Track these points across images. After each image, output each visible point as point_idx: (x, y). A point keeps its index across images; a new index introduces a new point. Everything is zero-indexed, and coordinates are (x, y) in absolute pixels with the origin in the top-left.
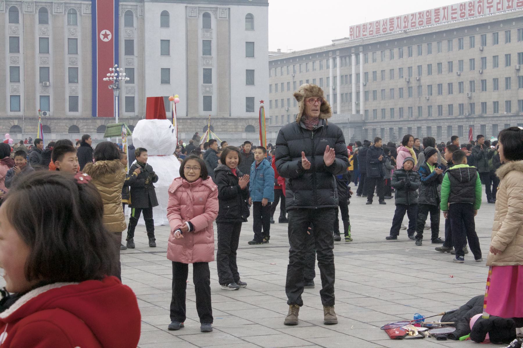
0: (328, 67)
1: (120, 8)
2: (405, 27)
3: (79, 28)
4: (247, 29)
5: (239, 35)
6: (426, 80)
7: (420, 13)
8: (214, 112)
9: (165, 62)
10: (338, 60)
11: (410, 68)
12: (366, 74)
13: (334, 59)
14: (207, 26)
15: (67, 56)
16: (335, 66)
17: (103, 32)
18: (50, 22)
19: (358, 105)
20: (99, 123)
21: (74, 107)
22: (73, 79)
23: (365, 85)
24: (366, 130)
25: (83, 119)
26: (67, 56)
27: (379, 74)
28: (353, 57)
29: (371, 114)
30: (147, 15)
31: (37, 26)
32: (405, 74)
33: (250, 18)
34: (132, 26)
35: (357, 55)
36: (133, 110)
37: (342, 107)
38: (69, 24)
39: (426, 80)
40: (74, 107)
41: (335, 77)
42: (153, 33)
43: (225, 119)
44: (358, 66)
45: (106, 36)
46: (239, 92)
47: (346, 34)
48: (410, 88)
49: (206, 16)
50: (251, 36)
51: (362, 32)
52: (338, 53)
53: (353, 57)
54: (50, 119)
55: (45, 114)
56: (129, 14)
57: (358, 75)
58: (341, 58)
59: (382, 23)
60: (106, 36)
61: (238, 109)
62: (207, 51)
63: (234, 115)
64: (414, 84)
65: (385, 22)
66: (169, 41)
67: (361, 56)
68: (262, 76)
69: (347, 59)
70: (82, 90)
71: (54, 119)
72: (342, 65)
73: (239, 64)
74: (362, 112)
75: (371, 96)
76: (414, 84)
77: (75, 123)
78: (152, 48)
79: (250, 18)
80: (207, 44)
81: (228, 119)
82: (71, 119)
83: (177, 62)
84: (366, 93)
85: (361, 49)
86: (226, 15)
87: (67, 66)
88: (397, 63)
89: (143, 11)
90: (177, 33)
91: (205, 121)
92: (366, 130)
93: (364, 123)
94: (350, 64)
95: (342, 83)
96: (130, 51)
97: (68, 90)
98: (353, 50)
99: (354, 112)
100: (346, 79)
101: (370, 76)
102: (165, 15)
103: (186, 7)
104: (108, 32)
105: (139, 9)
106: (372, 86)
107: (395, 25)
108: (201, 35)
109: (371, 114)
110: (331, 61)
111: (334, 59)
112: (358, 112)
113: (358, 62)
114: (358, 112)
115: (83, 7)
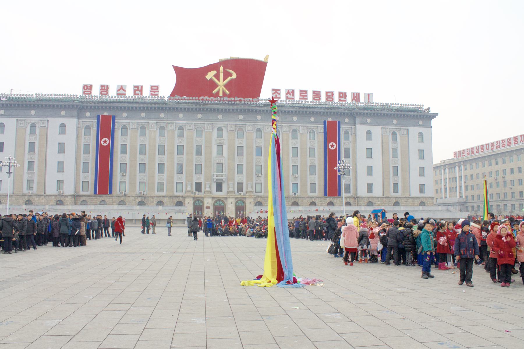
0: (440, 174)
1: (341, 129)
2: (492, 149)
3: (316, 141)
4: (419, 142)
5: (414, 146)
6: (509, 177)
7: (502, 141)
8: (399, 194)
9: (369, 162)
10: (447, 169)
11: (497, 172)
12: (466, 177)
13: (444, 170)
14: (394, 140)
15: (309, 159)
16: (445, 173)
17: (331, 144)
18: (299, 138)
19: (460, 193)
20: (329, 200)
21: (313, 190)
22: (313, 173)
23: (465, 182)
24: (467, 207)
25: (319, 197)
26: (309, 159)
27: (475, 176)
28: (457, 168)
29: (470, 198)
30: (358, 133)
31: (291, 140)
32: (494, 175)
33: (421, 134)
34: (349, 140)
35: (460, 166)
36: (350, 193)
37: (450, 194)
38: (310, 139)
39: (509, 177)
40: (313, 190)
41: (445, 179)
42: (362, 144)
43: (406, 197)
44: (461, 173)
45: (333, 146)
46: (415, 181)
47: (452, 157)
48: (497, 183)
49: (394, 134)
50: (422, 146)
51: (462, 155)
52: (447, 166)
53: (457, 168)
54: (298, 197)
55: (295, 194)
56: (346, 132)
57: (460, 177)
58: (449, 169)
59: (475, 149)
60: (332, 146)
61: (415, 192)
62: (395, 156)
63: (413, 195)
64: (500, 180)
65: (477, 148)
66: (371, 149)
67: (462, 166)
68: (429, 172)
69: (453, 169)
70: (318, 179)
71: (301, 197)
72: (449, 172)
73: (415, 163)
74: (463, 197)
75: (469, 188)
76: (500, 180)
77: (313, 200)
78: (361, 153)
79: (421, 134)
80: (395, 150)
81: (408, 198)
82: (311, 198)
83: (377, 162)
84: (466, 187)
85: (462, 163)
86: (406, 133)
87: (309, 165)
88: (487, 169)
89: (355, 130)
90: (376, 144)
91: (394, 199)
92: (467, 207)
93: (466, 203)
94: (455, 172)
95: (450, 181)
96: (347, 156)
97: (310, 179)
98: (457, 164)
99: (458, 197)
100: (453, 179)
101: (469, 177)
102: (369, 133)
103: (382, 128)
104: (334, 144)
105: (353, 130)
106: (470, 183)
107: (485, 149)
108: (391, 146)
109: (470, 198)
110: (442, 171)
111: (444, 170)
112: (461, 197)
113: (460, 170)
114: (461, 197)
115: (319, 128)
